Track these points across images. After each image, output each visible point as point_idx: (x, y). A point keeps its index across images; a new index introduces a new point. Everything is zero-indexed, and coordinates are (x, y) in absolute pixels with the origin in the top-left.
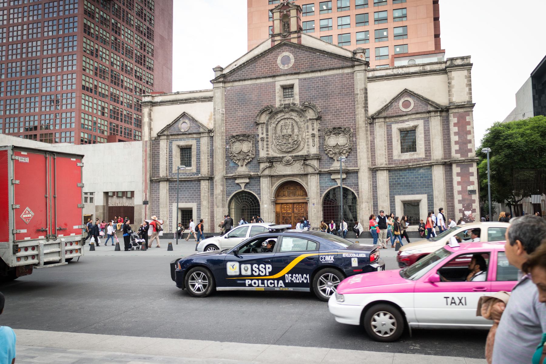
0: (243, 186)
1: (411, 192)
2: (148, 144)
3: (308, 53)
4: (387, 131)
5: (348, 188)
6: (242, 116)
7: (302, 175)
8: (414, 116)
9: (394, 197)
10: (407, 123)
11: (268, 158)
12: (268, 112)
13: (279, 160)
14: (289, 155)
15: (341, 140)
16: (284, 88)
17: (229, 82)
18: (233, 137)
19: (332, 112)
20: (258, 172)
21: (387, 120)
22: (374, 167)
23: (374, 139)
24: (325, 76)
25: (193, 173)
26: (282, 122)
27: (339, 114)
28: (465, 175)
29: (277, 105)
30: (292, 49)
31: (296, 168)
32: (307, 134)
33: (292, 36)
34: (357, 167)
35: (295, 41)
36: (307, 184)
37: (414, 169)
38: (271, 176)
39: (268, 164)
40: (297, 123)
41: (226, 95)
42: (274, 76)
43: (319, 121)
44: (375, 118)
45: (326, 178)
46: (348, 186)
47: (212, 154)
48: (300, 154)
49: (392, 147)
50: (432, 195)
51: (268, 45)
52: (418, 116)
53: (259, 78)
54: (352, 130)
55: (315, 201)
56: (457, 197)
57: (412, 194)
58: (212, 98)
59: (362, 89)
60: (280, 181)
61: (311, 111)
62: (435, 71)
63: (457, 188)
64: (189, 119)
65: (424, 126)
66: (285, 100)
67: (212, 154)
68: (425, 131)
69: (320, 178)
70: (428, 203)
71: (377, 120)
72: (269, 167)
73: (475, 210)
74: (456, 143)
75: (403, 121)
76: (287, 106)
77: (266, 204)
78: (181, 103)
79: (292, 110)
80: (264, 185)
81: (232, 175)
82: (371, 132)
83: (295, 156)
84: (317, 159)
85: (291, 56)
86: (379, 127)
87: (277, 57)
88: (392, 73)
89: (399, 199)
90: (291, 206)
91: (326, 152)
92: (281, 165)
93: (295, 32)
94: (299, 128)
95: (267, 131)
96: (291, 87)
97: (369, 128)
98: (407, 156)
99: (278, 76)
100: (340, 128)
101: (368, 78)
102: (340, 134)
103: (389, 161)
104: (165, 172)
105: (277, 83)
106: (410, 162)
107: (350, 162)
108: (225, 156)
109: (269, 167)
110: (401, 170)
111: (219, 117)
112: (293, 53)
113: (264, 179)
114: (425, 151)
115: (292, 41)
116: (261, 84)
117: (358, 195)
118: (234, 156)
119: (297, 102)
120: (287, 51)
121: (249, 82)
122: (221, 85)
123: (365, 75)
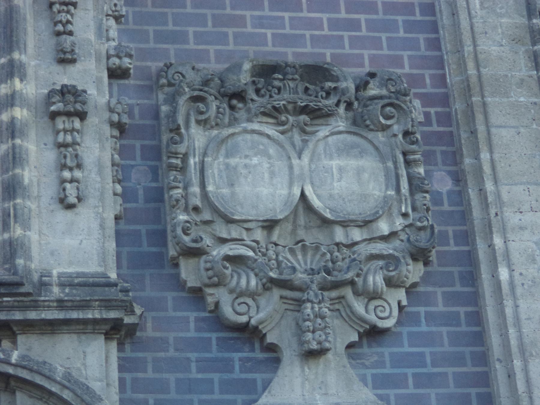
15: (346, 174)
54: (417, 109)
84: (116, 331)
91: (190, 272)
100: (316, 73)
102: (318, 115)
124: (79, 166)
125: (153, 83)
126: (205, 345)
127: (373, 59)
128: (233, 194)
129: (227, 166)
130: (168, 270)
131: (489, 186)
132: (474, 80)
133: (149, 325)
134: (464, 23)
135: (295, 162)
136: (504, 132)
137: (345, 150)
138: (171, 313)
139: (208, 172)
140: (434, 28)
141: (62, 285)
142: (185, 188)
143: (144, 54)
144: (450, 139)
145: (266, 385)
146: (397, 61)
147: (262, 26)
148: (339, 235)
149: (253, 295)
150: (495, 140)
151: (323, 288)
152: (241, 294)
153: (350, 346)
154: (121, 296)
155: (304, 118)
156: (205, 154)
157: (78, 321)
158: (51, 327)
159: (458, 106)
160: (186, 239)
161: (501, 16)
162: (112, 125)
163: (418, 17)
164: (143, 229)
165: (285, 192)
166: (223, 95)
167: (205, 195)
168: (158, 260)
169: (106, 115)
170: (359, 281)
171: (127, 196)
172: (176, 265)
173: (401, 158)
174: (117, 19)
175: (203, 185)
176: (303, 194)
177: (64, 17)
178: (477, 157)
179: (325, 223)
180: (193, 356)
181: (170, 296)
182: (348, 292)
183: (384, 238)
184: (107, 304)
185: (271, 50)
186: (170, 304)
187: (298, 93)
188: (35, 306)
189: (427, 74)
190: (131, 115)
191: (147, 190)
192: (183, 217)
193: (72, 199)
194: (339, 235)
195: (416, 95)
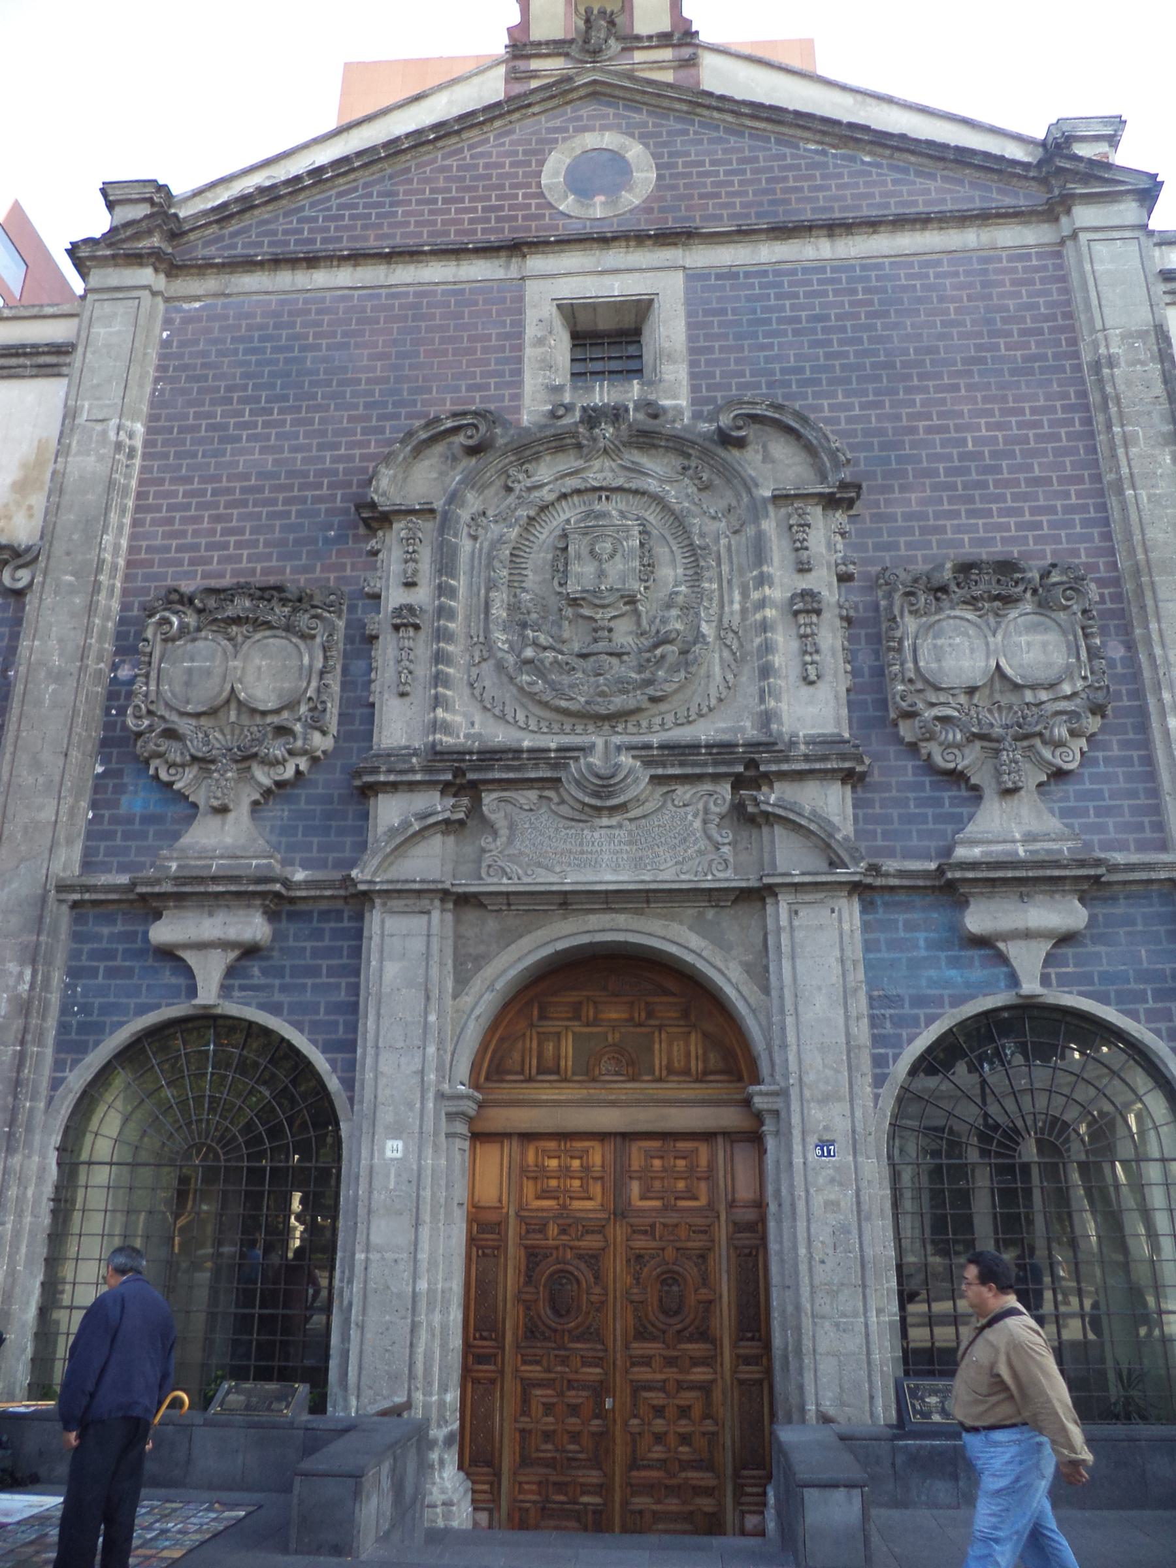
0: (209, 974)
3: (746, 142)
5: (1110, 1014)
6: (262, 475)
12: (460, 439)
13: (539, 773)
15: (1033, 647)
17: (204, 268)
18: (178, 600)
19: (931, 473)
20: (353, 864)
24: (869, 265)
26: (568, 513)
27: (983, 485)
31: (671, 843)
32: (755, 595)
33: (639, 56)
35: (668, 77)
36: (760, 974)
38: (463, 901)
39: (439, 805)
40: (678, 522)
41: (166, 344)
42: (516, 248)
43: (840, 517)
45: (917, 928)
46: (1103, 999)
48: (704, 731)
53: (412, 255)
54: (1093, 591)
58: (62, 350)
59: (1142, 335)
60: (526, 943)
61: (782, 450)
69: (866, 927)
77: (397, 1132)
80: (392, 970)
81: (124, 879)
84: (849, 777)
85: (635, 152)
87: (539, 154)
90: (597, 1155)
92: (544, 818)
93: (664, 39)
94: (694, 554)
95: (446, 564)
99: (540, 245)
100: (1006, 567)
102: (1008, 601)
105: (531, 287)
108: (98, 734)
109: (449, 826)
112: (643, 138)
113: (394, 924)
116: (424, 292)
118: (171, 734)
120: (603, 128)
121: (345, 276)
124: (817, 652)
125: (873, 584)
126: (920, 786)
127: (1054, 552)
128: (940, 668)
129: (935, 646)
130: (889, 730)
131: (1158, 651)
132: (1143, 563)
133: (876, 772)
134: (1134, 516)
135: (991, 639)
136: (1170, 605)
137: (1031, 628)
138: (893, 763)
139: (920, 652)
140: (1106, 522)
141: (807, 744)
142: (902, 665)
143: (866, 562)
144: (1121, 614)
145: (971, 817)
146: (1075, 553)
147: (960, 532)
148: (1029, 696)
149: (959, 746)
150: (1162, 613)
151: (1017, 739)
152: (949, 746)
153: (1040, 785)
154: (853, 750)
155: (997, 604)
156: (916, 637)
157: (820, 771)
158: (799, 776)
159: (1129, 586)
160: (904, 704)
161: (1167, 507)
162: (842, 618)
163: (1093, 515)
164: (869, 698)
165: (983, 664)
166: (930, 590)
167: (917, 669)
168: (882, 722)
169: (837, 611)
170: (1047, 733)
171: (855, 673)
172: (896, 725)
173: (1080, 632)
174: (843, 535)
175: (916, 662)
176: (998, 665)
177: (800, 536)
178: (1147, 627)
179: (1017, 687)
180: (911, 795)
181: (892, 749)
182: (1037, 742)
183: (1067, 698)
184: (843, 757)
185: (968, 551)
186: (892, 756)
187: (991, 584)
188: (787, 759)
189: (1101, 561)
190: (856, 609)
191: (870, 667)
192: (900, 688)
193: (813, 677)
194: (1029, 696)
195: (1092, 580)
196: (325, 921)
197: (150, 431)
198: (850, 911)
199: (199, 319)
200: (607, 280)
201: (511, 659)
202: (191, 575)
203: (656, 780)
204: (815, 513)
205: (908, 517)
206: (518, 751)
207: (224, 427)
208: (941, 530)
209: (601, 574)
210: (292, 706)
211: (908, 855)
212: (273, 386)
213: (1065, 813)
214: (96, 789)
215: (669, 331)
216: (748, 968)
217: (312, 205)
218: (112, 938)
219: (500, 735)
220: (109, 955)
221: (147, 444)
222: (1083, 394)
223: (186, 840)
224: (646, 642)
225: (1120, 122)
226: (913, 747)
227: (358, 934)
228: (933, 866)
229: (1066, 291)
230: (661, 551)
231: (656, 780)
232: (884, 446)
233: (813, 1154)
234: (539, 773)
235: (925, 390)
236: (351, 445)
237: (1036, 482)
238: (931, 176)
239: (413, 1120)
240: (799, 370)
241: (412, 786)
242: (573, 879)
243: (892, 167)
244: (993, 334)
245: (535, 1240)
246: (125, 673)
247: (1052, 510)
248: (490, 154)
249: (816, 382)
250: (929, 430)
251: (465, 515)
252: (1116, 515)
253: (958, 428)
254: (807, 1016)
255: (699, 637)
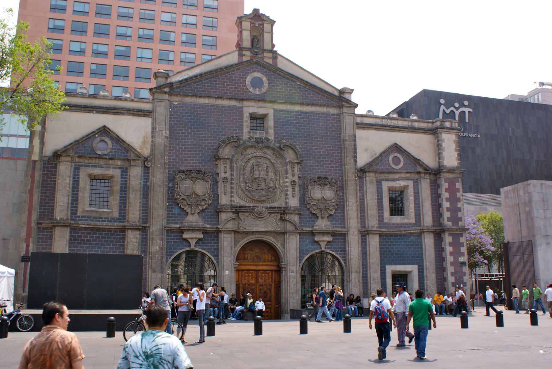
0: (193, 243)
1: (402, 262)
2: (38, 166)
3: (286, 80)
4: (377, 188)
7: (276, 233)
8: (403, 175)
9: (385, 267)
10: (398, 182)
11: (232, 206)
13: (250, 210)
14: (262, 205)
15: (329, 193)
16: (253, 117)
21: (377, 175)
22: (364, 229)
23: (363, 196)
25: (113, 219)
26: (253, 161)
27: (323, 161)
28: (456, 244)
29: (245, 136)
30: (265, 70)
33: (266, 54)
34: (344, 228)
36: (283, 245)
37: (405, 235)
38: (236, 232)
39: (234, 216)
41: (171, 112)
42: (242, 100)
43: (299, 165)
44: (366, 172)
45: (308, 240)
46: (333, 251)
47: (146, 192)
48: (276, 205)
49: (382, 207)
50: (423, 266)
51: (233, 59)
52: (408, 175)
55: (294, 268)
56: (450, 269)
57: (404, 264)
61: (291, 152)
62: (423, 129)
63: (450, 259)
64: (112, 138)
65: (414, 187)
66: (256, 133)
67: (146, 192)
68: (414, 193)
70: (419, 275)
71: (367, 174)
72: (234, 219)
73: (466, 283)
74: (448, 209)
75: (393, 180)
76: (259, 141)
78: (97, 112)
79: (268, 147)
80: (225, 243)
82: (360, 187)
83: (271, 207)
84: (299, 214)
85: (264, 79)
86: (370, 182)
88: (381, 123)
89: (390, 269)
94: (276, 171)
96: (262, 118)
97: (358, 183)
98: (397, 219)
99: (247, 100)
101: (357, 124)
103: (379, 224)
104: (65, 212)
105: (245, 109)
106: (401, 227)
107: (336, 221)
110: (391, 236)
111: (160, 141)
112: (266, 75)
113: (225, 236)
114: (415, 215)
115: (266, 60)
117: (345, 263)
118: (183, 199)
119: (272, 138)
120: (258, 72)
121: (206, 101)
122: (167, 97)
123: (354, 120)
126: (309, 215)
137: (329, 190)
140: (342, 170)
144: (343, 187)
158: (291, 213)
181: (305, 209)
196: (212, 236)
197: (170, 132)
198: (298, 237)
199: (177, 107)
200: (259, 109)
201: (244, 189)
202: (181, 166)
203: (269, 213)
204: (296, 165)
205: (311, 166)
206: (246, 207)
207: (185, 133)
208: (315, 169)
209: (260, 174)
210: (205, 195)
211: (307, 227)
212: (194, 125)
213: (331, 221)
214: (168, 208)
215: (270, 122)
216: (281, 244)
217: (199, 82)
218: (174, 236)
219: (242, 203)
220: (174, 239)
221: (170, 135)
222: (341, 145)
223: (187, 219)
224: (267, 187)
225: (353, 90)
226: (309, 209)
227: (218, 237)
228: (311, 229)
229: (340, 123)
230: (270, 170)
231: (269, 213)
232: (307, 151)
233: (291, 274)
234: (250, 210)
235: (315, 141)
236: (211, 140)
237: (331, 161)
238: (319, 94)
239: (230, 268)
240: (293, 134)
241: (227, 211)
242: (255, 229)
243: (312, 91)
244: (327, 130)
245: (244, 287)
246: (171, 185)
247: (333, 167)
248: (235, 74)
249: (296, 137)
250: (315, 149)
251: (235, 159)
252: (344, 170)
253: (320, 149)
254: (291, 253)
255: (276, 187)
